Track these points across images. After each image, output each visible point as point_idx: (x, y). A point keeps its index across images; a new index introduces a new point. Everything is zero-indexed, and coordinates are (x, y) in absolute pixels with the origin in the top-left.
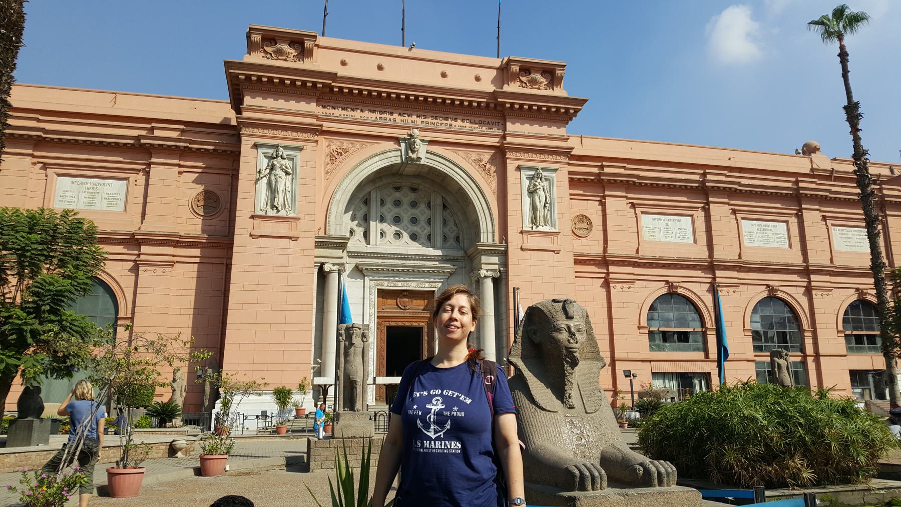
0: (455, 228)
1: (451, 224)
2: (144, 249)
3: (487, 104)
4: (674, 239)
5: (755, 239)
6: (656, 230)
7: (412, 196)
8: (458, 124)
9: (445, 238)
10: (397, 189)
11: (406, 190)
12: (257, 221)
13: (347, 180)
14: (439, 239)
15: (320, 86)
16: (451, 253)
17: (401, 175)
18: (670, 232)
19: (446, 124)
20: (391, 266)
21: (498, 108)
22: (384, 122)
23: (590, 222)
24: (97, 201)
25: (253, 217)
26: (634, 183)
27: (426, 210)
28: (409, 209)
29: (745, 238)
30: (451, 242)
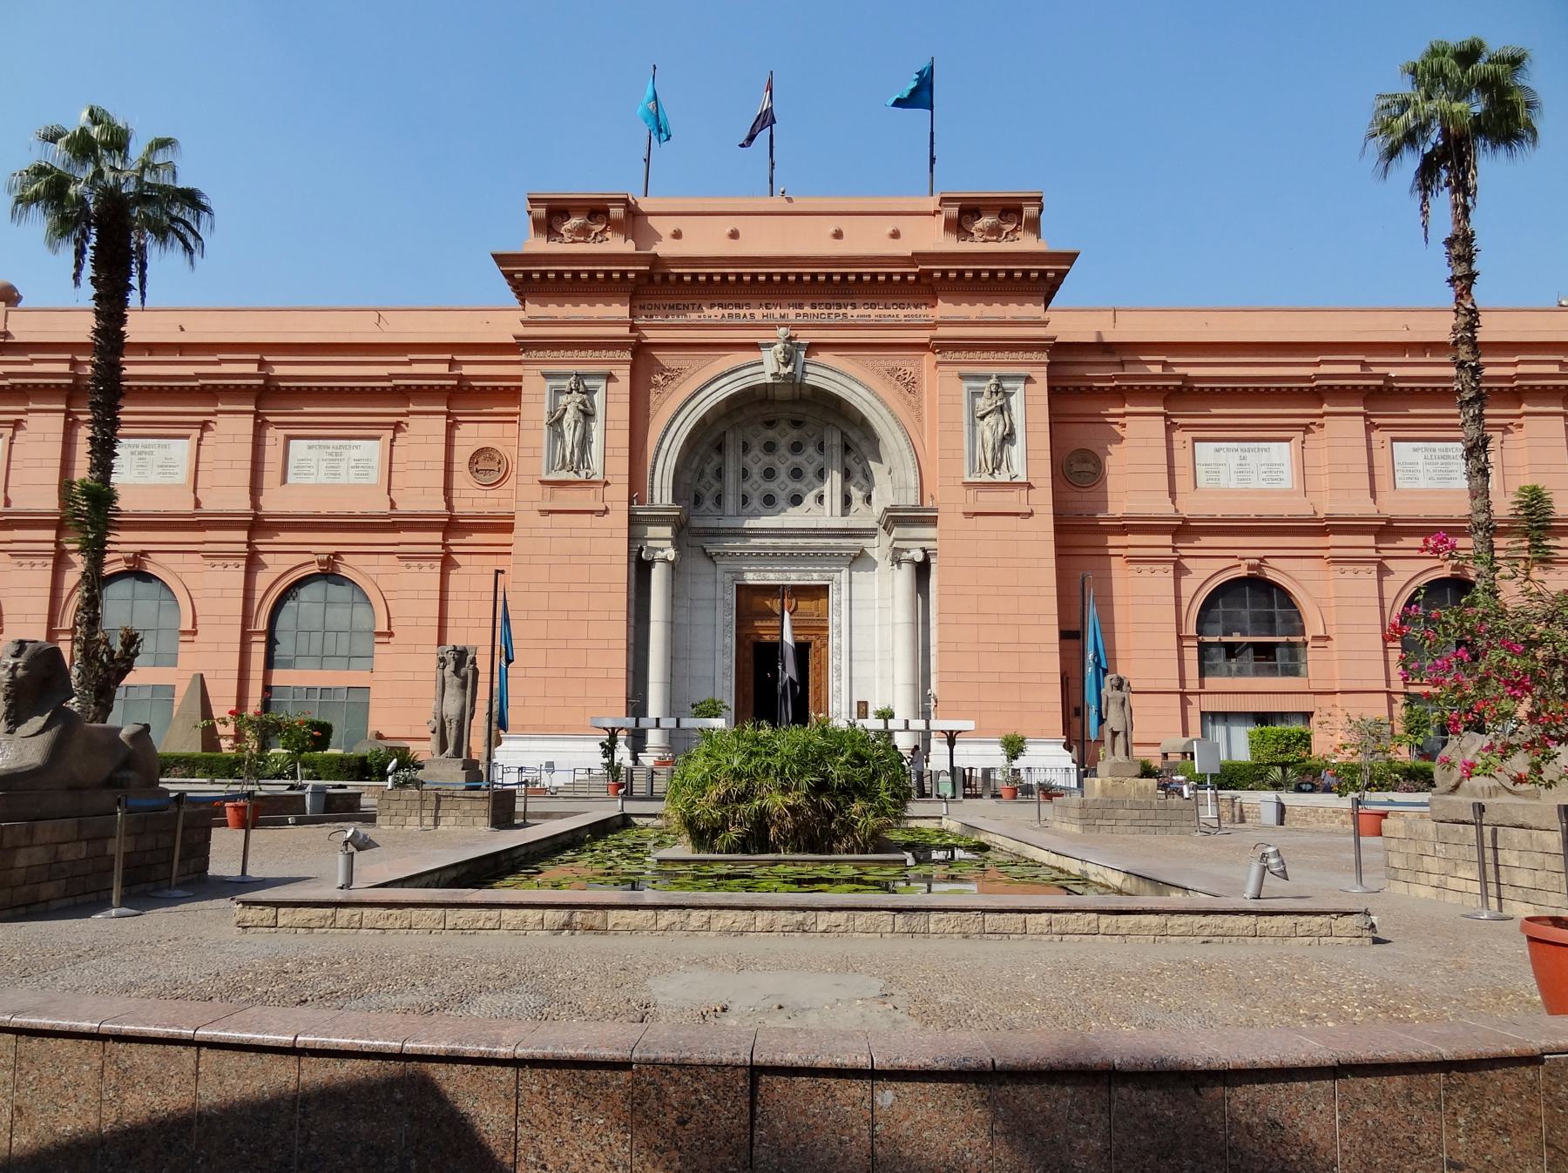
0: (863, 482)
1: (858, 477)
4: (1256, 483)
6: (1222, 468)
7: (794, 434)
8: (855, 314)
9: (847, 500)
10: (770, 424)
11: (783, 425)
12: (548, 489)
15: (631, 276)
17: (773, 402)
18: (1243, 471)
19: (837, 315)
20: (755, 547)
21: (924, 281)
22: (735, 321)
24: (343, 471)
25: (542, 482)
27: (816, 455)
28: (788, 455)
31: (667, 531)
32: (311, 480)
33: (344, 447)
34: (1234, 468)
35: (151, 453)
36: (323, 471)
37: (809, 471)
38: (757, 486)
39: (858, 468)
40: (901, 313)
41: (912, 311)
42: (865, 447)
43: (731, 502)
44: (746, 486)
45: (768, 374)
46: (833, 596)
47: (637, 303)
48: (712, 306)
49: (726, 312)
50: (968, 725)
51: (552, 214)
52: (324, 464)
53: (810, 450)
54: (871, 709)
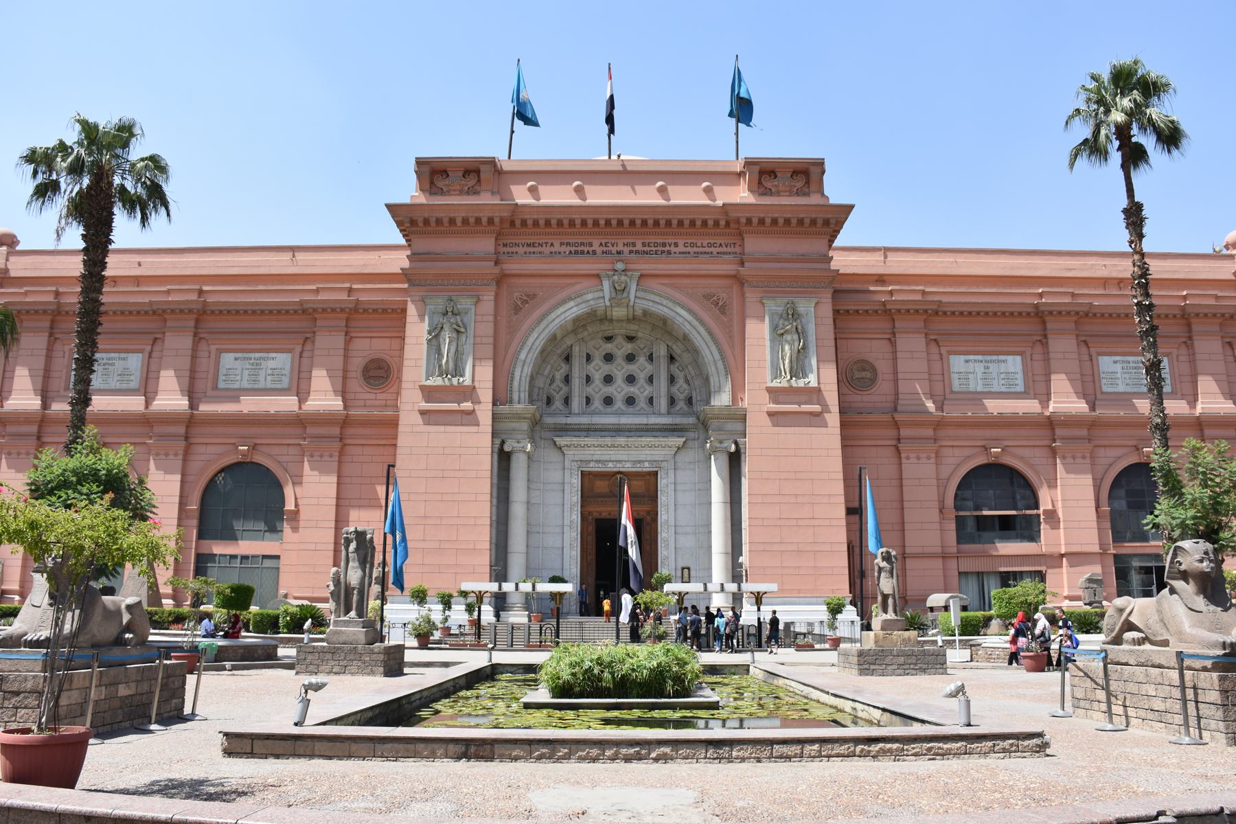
0: (685, 386)
2: (311, 430)
3: (716, 223)
5: (1119, 382)
6: (971, 376)
7: (629, 348)
9: (672, 401)
10: (609, 339)
11: (620, 340)
13: (535, 335)
14: (663, 403)
16: (678, 420)
17: (611, 321)
19: (663, 252)
21: (732, 225)
23: (874, 370)
24: (261, 378)
26: (936, 313)
28: (623, 363)
29: (1104, 381)
30: (681, 405)
31: (525, 426)
32: (237, 386)
33: (263, 359)
34: (980, 376)
35: (113, 364)
36: (246, 377)
37: (642, 377)
38: (598, 390)
39: (681, 375)
40: (715, 250)
41: (724, 249)
42: (686, 358)
43: (576, 403)
44: (590, 390)
45: (607, 299)
46: (662, 482)
47: (501, 242)
48: (562, 244)
49: (573, 249)
50: (772, 587)
51: (433, 173)
52: (246, 373)
53: (642, 360)
54: (693, 573)
